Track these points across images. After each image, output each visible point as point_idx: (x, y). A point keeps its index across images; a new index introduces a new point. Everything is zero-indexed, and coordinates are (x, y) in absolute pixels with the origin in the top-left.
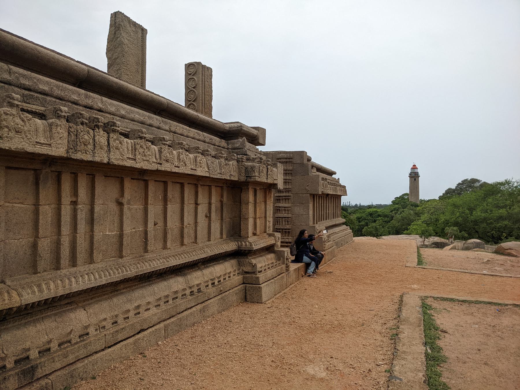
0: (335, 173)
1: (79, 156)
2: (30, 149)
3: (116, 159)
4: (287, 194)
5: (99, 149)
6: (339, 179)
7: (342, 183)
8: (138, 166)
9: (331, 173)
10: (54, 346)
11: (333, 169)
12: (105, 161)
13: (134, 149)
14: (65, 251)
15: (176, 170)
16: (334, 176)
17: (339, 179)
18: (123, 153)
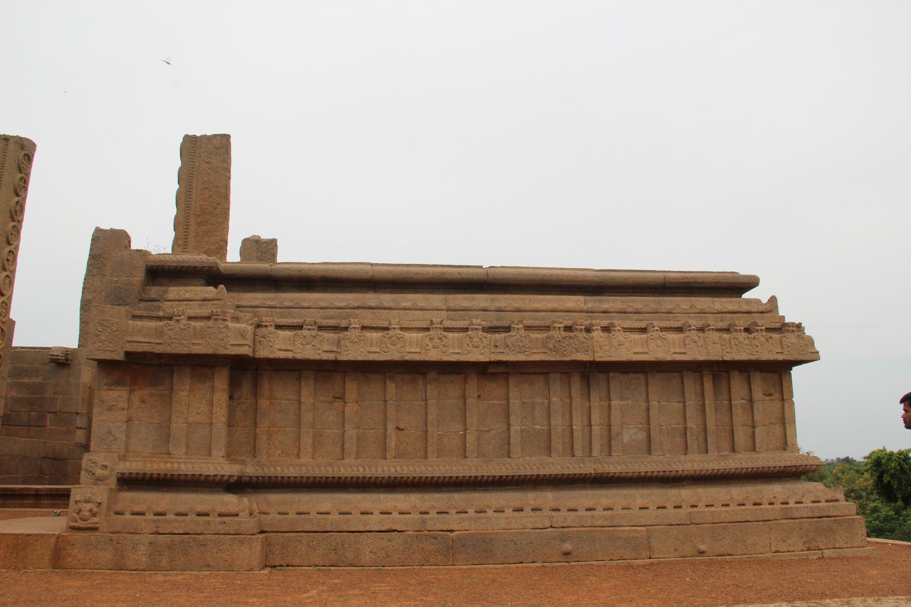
0: (751, 283)
6: (773, 300)
7: (789, 312)
11: (744, 270)
16: (746, 296)
17: (773, 300)
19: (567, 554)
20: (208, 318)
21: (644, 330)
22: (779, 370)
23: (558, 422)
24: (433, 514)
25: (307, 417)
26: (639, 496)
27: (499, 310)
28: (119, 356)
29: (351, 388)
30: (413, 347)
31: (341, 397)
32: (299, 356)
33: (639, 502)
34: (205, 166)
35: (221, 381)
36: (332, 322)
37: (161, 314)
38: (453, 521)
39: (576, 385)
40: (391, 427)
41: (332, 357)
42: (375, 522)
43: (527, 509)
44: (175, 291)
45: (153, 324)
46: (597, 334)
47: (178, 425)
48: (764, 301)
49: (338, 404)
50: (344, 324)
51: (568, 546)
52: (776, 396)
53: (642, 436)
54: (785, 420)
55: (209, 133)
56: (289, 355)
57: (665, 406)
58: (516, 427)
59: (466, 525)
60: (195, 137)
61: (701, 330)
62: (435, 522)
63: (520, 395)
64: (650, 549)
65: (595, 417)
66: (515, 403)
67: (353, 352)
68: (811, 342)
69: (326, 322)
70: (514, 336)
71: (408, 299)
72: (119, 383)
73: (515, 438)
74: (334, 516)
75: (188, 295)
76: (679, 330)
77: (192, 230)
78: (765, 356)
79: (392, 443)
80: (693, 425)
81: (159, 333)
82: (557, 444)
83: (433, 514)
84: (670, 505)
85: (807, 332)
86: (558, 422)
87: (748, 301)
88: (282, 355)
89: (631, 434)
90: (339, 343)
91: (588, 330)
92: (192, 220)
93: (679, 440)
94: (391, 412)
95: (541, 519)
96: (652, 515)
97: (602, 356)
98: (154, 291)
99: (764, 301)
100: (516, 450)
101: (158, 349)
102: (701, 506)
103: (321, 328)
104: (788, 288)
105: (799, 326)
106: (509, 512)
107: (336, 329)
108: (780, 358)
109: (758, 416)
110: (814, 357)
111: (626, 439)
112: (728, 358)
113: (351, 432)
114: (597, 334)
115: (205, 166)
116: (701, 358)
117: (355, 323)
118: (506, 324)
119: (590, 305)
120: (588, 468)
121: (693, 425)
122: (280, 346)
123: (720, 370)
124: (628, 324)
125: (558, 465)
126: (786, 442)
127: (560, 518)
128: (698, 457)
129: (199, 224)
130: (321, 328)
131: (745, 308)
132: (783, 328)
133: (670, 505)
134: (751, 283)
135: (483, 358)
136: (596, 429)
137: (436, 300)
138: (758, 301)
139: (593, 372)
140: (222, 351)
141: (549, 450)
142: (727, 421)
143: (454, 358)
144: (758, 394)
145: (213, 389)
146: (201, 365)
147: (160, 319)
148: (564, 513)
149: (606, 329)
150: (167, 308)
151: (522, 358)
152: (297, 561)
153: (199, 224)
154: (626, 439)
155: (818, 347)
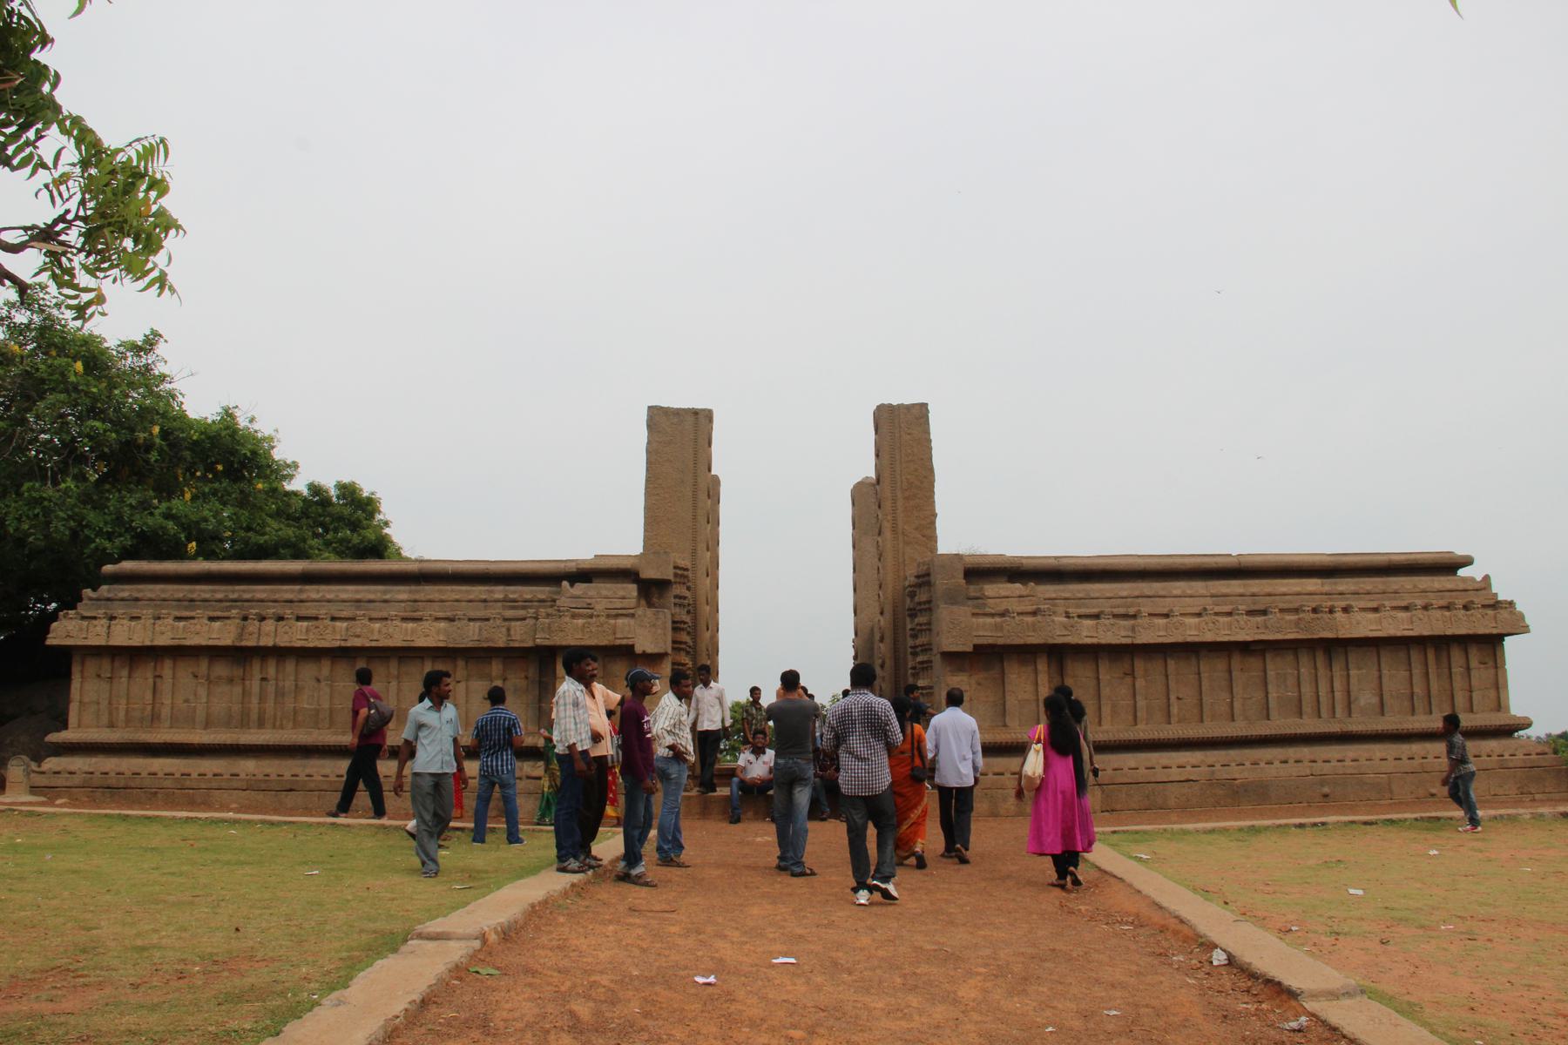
0: (1467, 562)
1: (244, 643)
2: (204, 643)
3: (283, 641)
4: (925, 658)
5: (268, 635)
6: (1487, 578)
8: (311, 645)
9: (1447, 566)
10: (210, 776)
11: (1460, 551)
12: (270, 644)
13: (308, 630)
14: (254, 716)
15: (374, 644)
16: (1462, 572)
17: (1487, 578)
18: (297, 635)
19: (1326, 796)
20: (1034, 613)
21: (1376, 610)
22: (1493, 643)
23: (1307, 690)
24: (1218, 766)
25: (1105, 691)
26: (1378, 750)
27: (1253, 595)
28: (969, 648)
29: (1140, 665)
30: (1192, 631)
31: (1132, 674)
32: (1103, 642)
33: (1379, 755)
34: (903, 434)
35: (1042, 665)
36: (1122, 611)
37: (988, 610)
38: (1234, 771)
39: (1321, 659)
40: (1173, 698)
41: (1128, 641)
42: (1175, 774)
43: (1291, 761)
44: (992, 589)
45: (989, 620)
46: (1339, 615)
47: (1011, 701)
48: (1479, 578)
49: (1128, 680)
50: (1132, 611)
51: (1326, 790)
52: (1491, 663)
53: (1375, 700)
54: (1498, 685)
55: (907, 402)
56: (1095, 641)
57: (1394, 675)
58: (1273, 695)
59: (1246, 774)
60: (890, 406)
61: (1425, 608)
62: (1223, 774)
63: (1276, 667)
64: (1391, 792)
65: (1337, 685)
66: (1271, 674)
67: (1144, 638)
68: (1521, 617)
69: (1116, 611)
70: (1272, 618)
71: (1178, 587)
72: (961, 670)
73: (1272, 704)
74: (1142, 771)
75: (1003, 593)
76: (1406, 608)
77: (900, 504)
78: (1481, 631)
79: (1174, 710)
80: (1418, 689)
81: (998, 627)
82: (1307, 707)
83: (1218, 766)
84: (1404, 757)
85: (1519, 607)
86: (1307, 690)
87: (1464, 580)
88: (1088, 641)
89: (1366, 698)
90: (1133, 629)
91: (1331, 612)
92: (899, 494)
93: (1407, 704)
94: (1172, 684)
95: (1305, 769)
96: (1390, 766)
97: (1343, 634)
98: (973, 590)
99: (1479, 578)
100: (1273, 714)
101: (1001, 641)
102: (1430, 757)
103: (1115, 616)
104: (1500, 566)
105: (1511, 603)
106: (1277, 764)
107: (1125, 616)
108: (1495, 631)
109: (1474, 682)
110: (1525, 629)
111: (1362, 702)
112: (1449, 632)
113: (1141, 703)
114: (1339, 615)
115: (903, 434)
116: (1426, 633)
117: (1145, 610)
118: (1262, 607)
119: (1327, 588)
120: (1335, 728)
121: (1418, 689)
122: (1087, 633)
123: (1441, 643)
124: (1362, 604)
125: (1309, 725)
126: (1500, 705)
127: (1319, 767)
128: (1423, 717)
129: (907, 498)
130: (1115, 616)
131: (1461, 586)
132: (1496, 605)
133: (1404, 757)
134: (1467, 562)
135: (1249, 638)
136: (1338, 695)
137: (1199, 586)
138: (1472, 579)
139: (1334, 648)
140: (1051, 641)
141: (1300, 714)
142: (1447, 686)
143: (1226, 639)
144: (1474, 663)
145: (1036, 672)
146: (1026, 653)
147: (992, 615)
148: (1320, 764)
149: (1346, 610)
150: (993, 606)
151: (1279, 637)
152: (1118, 807)
153: (907, 498)
154: (1362, 702)
155: (1528, 621)
